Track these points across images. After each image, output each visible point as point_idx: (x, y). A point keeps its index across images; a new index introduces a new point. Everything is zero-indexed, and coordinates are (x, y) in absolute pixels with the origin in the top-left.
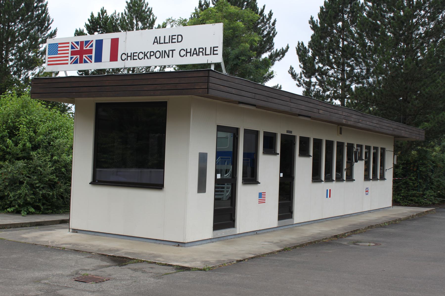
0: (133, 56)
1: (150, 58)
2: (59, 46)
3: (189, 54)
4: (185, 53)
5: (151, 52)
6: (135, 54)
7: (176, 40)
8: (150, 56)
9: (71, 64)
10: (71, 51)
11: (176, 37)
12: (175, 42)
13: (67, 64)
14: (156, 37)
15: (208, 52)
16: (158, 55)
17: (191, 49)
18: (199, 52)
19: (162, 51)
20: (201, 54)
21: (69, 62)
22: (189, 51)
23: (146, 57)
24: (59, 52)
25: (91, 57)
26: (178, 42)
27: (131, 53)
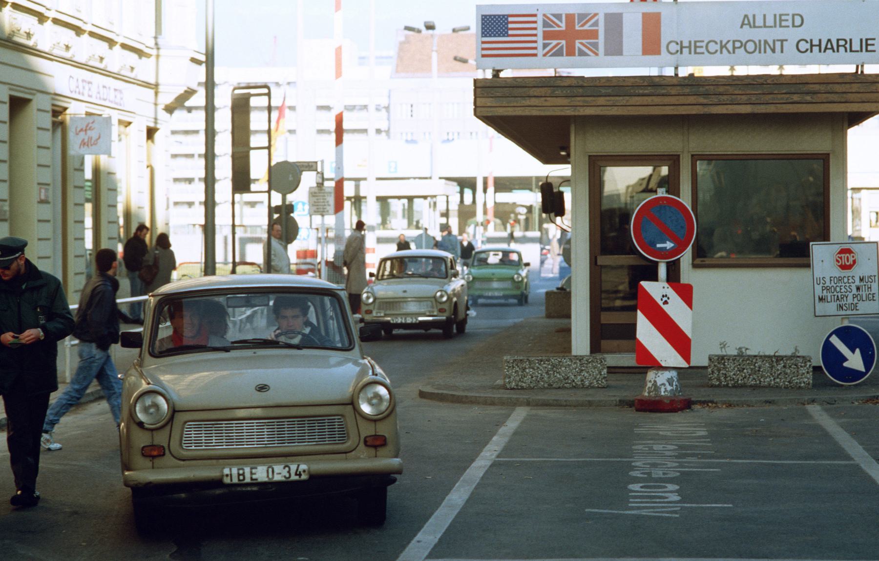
0: (694, 48)
1: (734, 52)
2: (510, 19)
3: (816, 49)
4: (808, 46)
5: (734, 42)
6: (698, 44)
7: (790, 23)
8: (734, 48)
9: (545, 55)
10: (544, 32)
11: (790, 18)
12: (788, 27)
13: (535, 55)
14: (746, 16)
15: (856, 46)
16: (750, 47)
17: (820, 41)
18: (838, 46)
19: (760, 41)
20: (842, 49)
21: (540, 52)
22: (816, 42)
23: (724, 50)
24: (510, 32)
25: (596, 45)
26: (794, 26)
27: (690, 42)
